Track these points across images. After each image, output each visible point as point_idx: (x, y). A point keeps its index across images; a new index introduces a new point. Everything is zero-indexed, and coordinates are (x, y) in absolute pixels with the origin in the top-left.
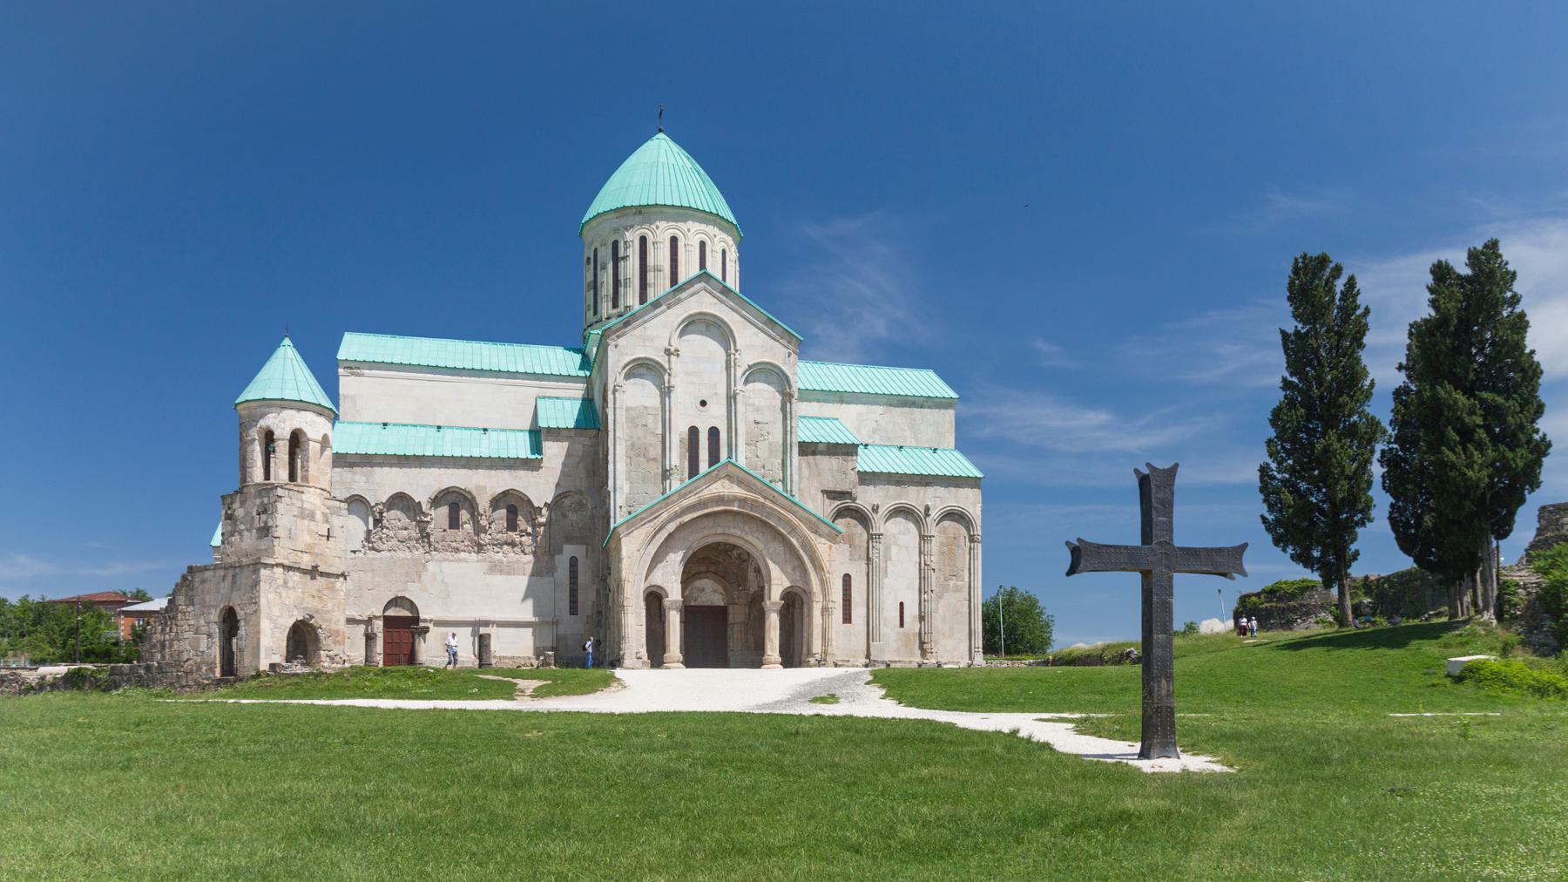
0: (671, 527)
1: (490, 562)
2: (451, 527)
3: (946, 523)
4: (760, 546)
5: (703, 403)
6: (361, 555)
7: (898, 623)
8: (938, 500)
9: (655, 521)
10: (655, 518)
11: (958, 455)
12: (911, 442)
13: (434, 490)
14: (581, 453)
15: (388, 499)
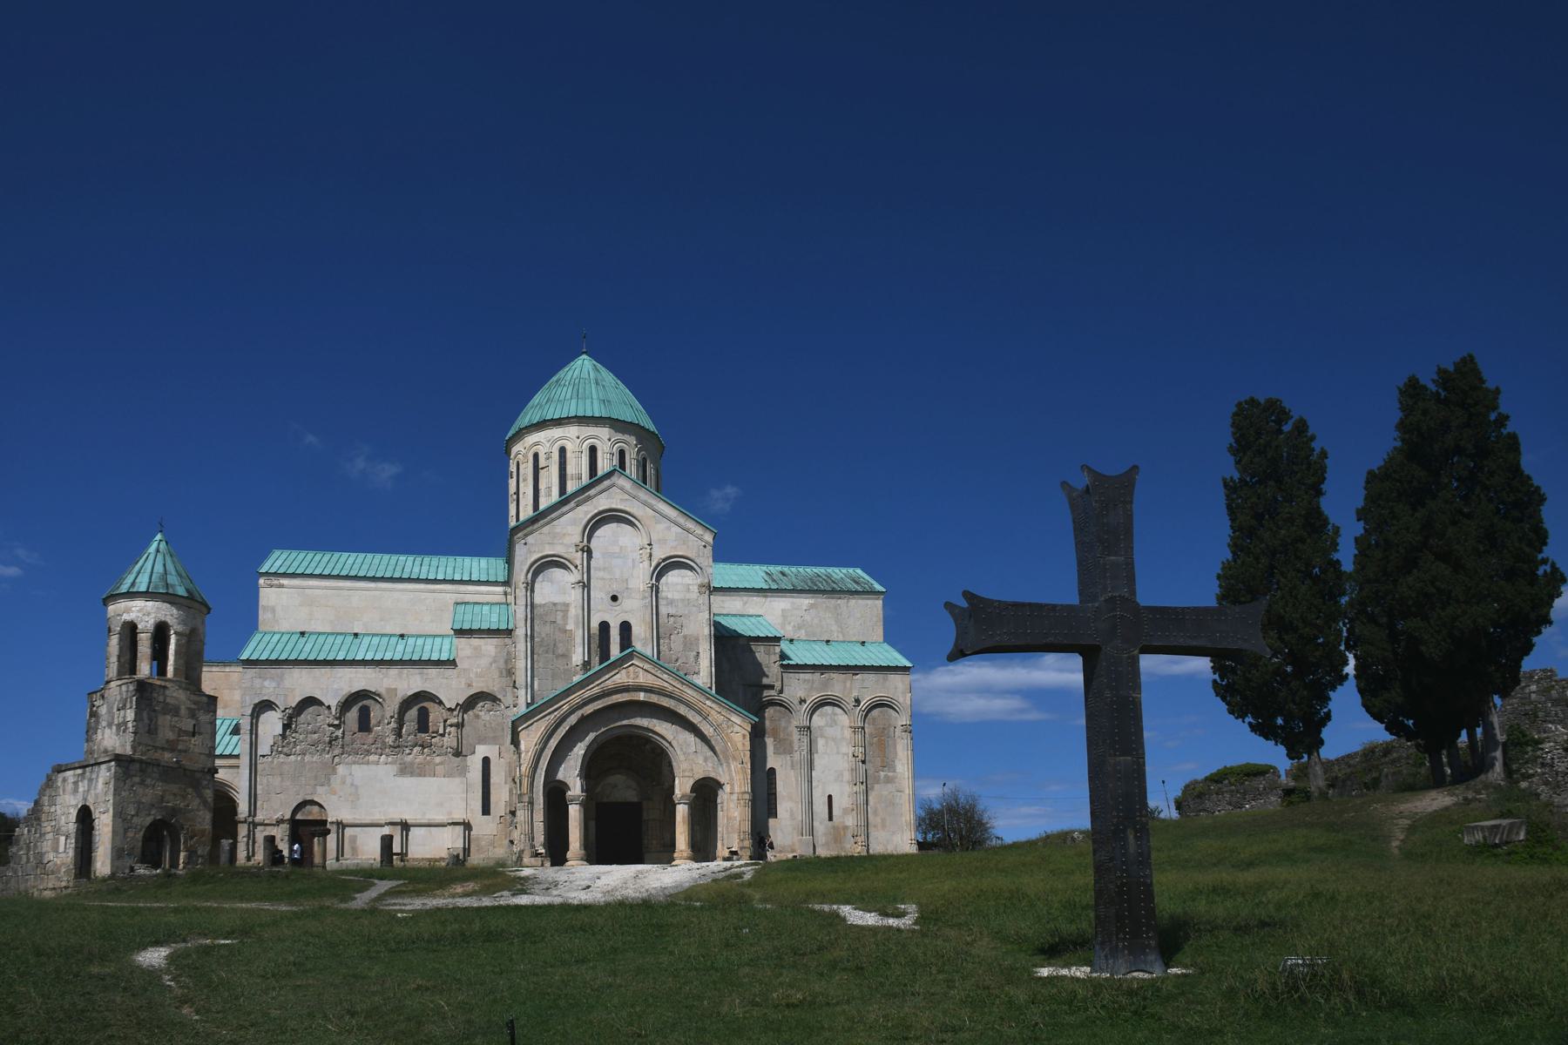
0: (573, 719)
1: (400, 764)
2: (360, 730)
3: (875, 712)
4: (670, 738)
5: (614, 598)
6: (270, 759)
7: (827, 816)
8: (869, 688)
9: (556, 713)
10: (555, 710)
11: (886, 646)
12: (838, 637)
13: (344, 693)
14: (493, 654)
15: (297, 705)
